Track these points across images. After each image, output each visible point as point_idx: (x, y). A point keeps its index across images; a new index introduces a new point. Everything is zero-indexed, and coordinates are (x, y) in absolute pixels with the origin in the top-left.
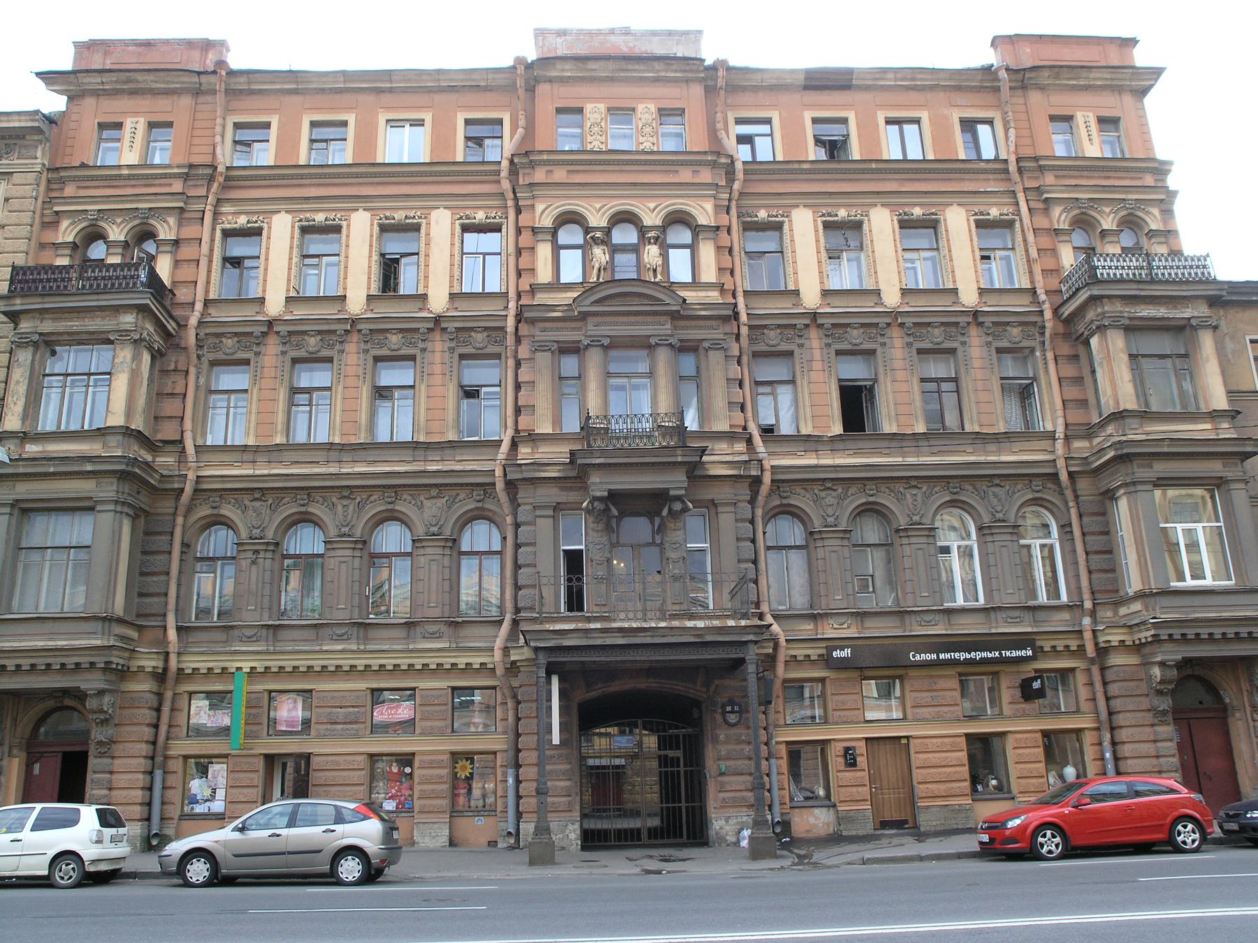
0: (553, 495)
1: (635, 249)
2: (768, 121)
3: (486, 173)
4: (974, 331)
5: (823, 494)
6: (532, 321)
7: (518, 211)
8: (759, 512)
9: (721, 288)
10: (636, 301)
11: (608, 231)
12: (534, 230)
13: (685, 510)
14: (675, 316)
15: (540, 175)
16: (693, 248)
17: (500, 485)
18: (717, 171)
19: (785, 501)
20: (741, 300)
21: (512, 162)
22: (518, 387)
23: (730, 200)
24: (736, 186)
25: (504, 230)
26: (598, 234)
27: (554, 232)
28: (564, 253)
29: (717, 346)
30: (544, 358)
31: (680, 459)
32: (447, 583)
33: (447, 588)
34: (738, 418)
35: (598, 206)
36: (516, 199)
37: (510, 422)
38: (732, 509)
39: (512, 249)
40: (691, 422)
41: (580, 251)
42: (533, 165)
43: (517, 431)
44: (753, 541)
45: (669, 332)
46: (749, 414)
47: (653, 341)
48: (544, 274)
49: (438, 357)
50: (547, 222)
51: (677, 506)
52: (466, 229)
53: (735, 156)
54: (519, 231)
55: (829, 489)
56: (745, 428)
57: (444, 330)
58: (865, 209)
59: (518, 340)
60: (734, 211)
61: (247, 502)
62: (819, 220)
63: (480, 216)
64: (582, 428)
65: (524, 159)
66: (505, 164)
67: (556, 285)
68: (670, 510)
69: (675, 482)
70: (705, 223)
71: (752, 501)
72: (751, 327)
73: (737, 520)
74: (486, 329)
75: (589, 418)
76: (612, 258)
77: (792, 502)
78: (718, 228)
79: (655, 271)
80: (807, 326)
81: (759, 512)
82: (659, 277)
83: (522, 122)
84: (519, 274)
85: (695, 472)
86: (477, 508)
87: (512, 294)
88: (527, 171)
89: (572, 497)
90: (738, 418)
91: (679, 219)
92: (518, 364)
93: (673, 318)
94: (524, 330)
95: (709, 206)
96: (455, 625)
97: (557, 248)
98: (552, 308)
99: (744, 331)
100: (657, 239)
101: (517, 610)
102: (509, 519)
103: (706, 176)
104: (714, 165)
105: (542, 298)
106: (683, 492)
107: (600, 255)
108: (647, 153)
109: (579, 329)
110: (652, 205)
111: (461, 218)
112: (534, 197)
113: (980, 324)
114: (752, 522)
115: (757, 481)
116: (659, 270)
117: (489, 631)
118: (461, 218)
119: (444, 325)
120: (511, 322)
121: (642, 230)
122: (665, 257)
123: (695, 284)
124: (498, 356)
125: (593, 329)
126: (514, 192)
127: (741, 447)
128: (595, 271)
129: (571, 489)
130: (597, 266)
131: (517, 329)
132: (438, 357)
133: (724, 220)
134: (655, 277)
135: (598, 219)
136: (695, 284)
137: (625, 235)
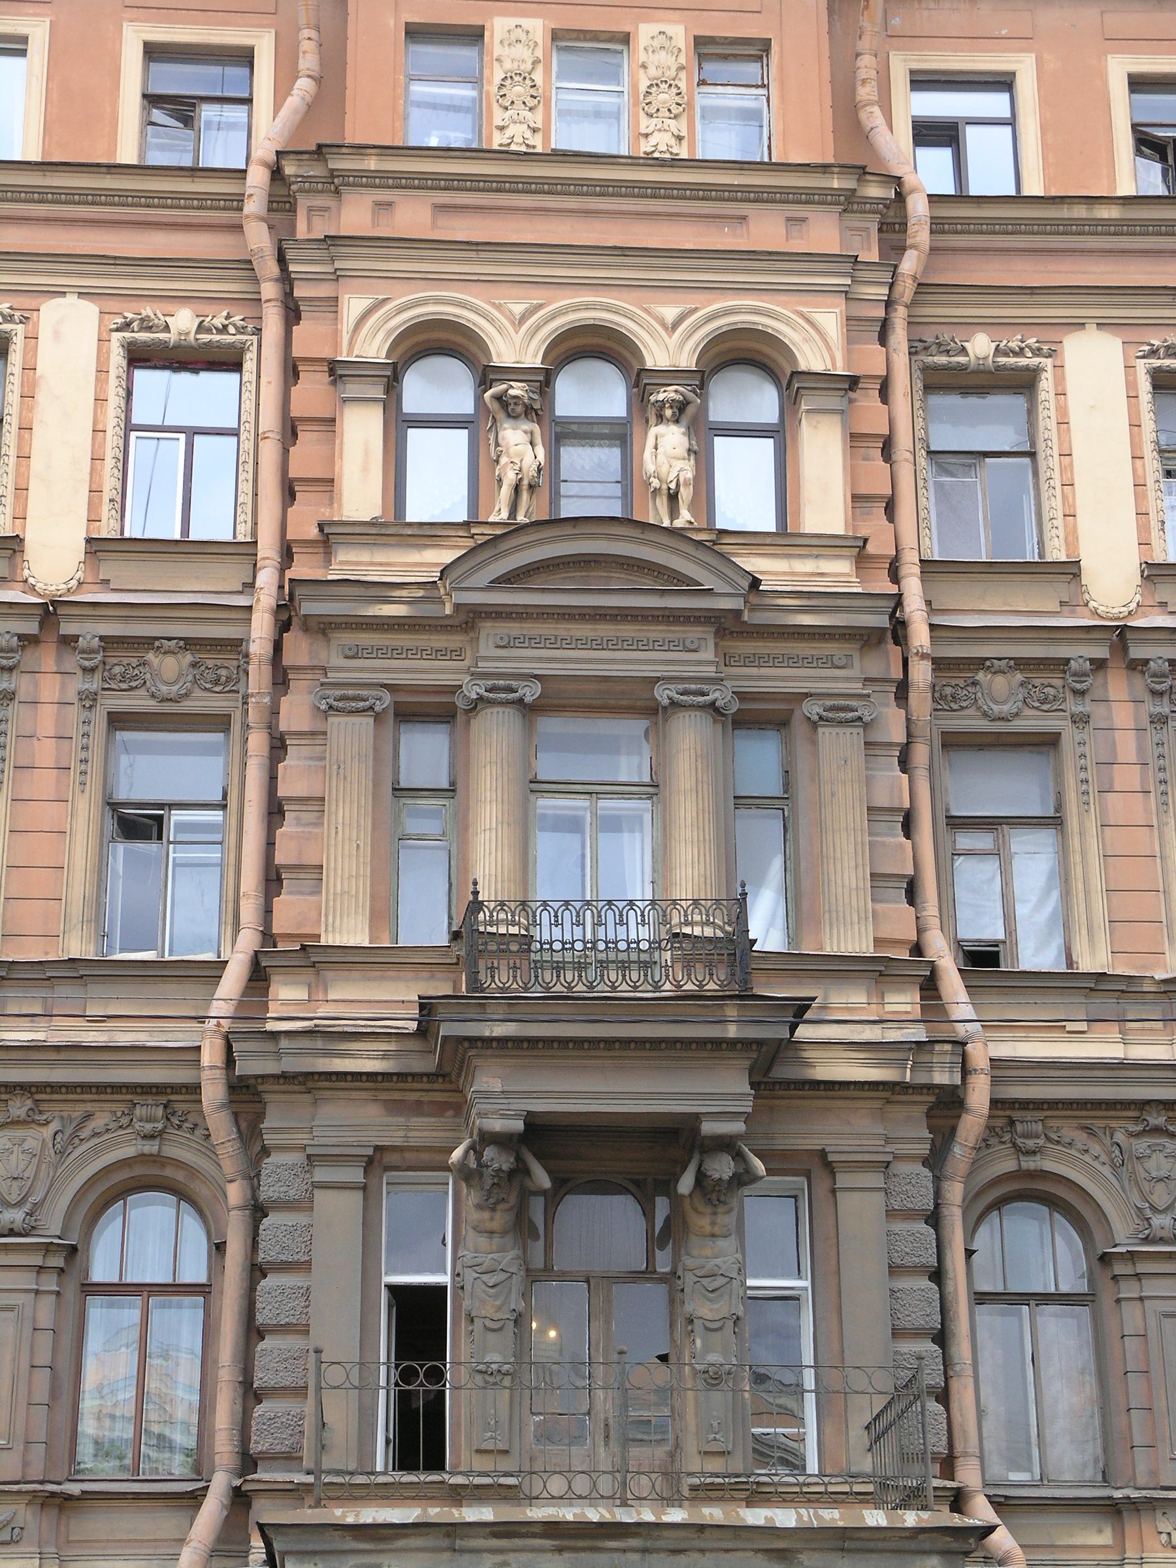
0: (365, 1122)
1: (618, 434)
2: (1003, 83)
3: (203, 201)
5: (1141, 1146)
6: (323, 628)
7: (292, 313)
8: (955, 1192)
9: (858, 550)
11: (544, 380)
12: (336, 371)
13: (743, 1178)
14: (726, 627)
15: (355, 215)
16: (781, 435)
17: (213, 1092)
18: (854, 221)
19: (1029, 1164)
20: (913, 588)
21: (276, 174)
22: (275, 811)
23: (889, 304)
24: (910, 264)
25: (249, 365)
26: (517, 389)
27: (392, 378)
28: (416, 437)
29: (842, 714)
30: (352, 734)
31: (732, 1031)
32: (42, 1378)
33: (41, 1393)
34: (899, 921)
35: (518, 309)
36: (286, 279)
37: (249, 911)
38: (876, 1180)
39: (270, 420)
40: (766, 928)
41: (464, 433)
42: (336, 185)
43: (268, 936)
44: (937, 1275)
45: (710, 671)
46: (931, 909)
47: (662, 694)
48: (360, 499)
49: (46, 720)
50: (373, 347)
51: (722, 1167)
52: (140, 357)
53: (909, 180)
54: (291, 370)
55: (1157, 1131)
56: (917, 949)
57: (69, 641)
59: (281, 678)
60: (899, 336)
62: (1142, 366)
63: (182, 323)
64: (456, 936)
65: (312, 167)
66: (258, 178)
67: (393, 529)
68: (701, 1177)
69: (717, 1096)
70: (818, 367)
71: (936, 1160)
72: (939, 664)
73: (891, 1214)
74: (189, 643)
75: (476, 906)
76: (554, 458)
77: (1049, 1165)
78: (853, 382)
79: (673, 497)
80: (1099, 665)
81: (955, 1192)
82: (685, 517)
83: (308, 61)
84: (289, 491)
85: (774, 1071)
86: (142, 1158)
87: (268, 549)
88: (319, 201)
89: (421, 1131)
90: (899, 921)
91: (743, 352)
92: (278, 747)
93: (722, 633)
94: (298, 650)
95: (830, 319)
96: (60, 1504)
97: (399, 425)
98: (382, 590)
99: (921, 673)
100: (681, 407)
101: (248, 1462)
102: (235, 1193)
103: (824, 233)
104: (849, 203)
105: (352, 562)
106: (738, 1127)
107: (520, 446)
108: (661, 163)
109: (457, 654)
110: (670, 313)
111: (126, 326)
112: (336, 277)
114: (934, 1219)
115: (947, 1104)
116: (685, 494)
117: (164, 1523)
118: (126, 326)
119: (68, 628)
120: (261, 629)
121: (641, 381)
122: (702, 458)
124: (221, 722)
125: (493, 652)
126: (282, 260)
127: (904, 1001)
128: (506, 492)
129: (418, 1108)
130: (510, 477)
131: (278, 647)
132: (46, 720)
133: (872, 360)
134: (674, 513)
135: (515, 347)
136: (785, 537)
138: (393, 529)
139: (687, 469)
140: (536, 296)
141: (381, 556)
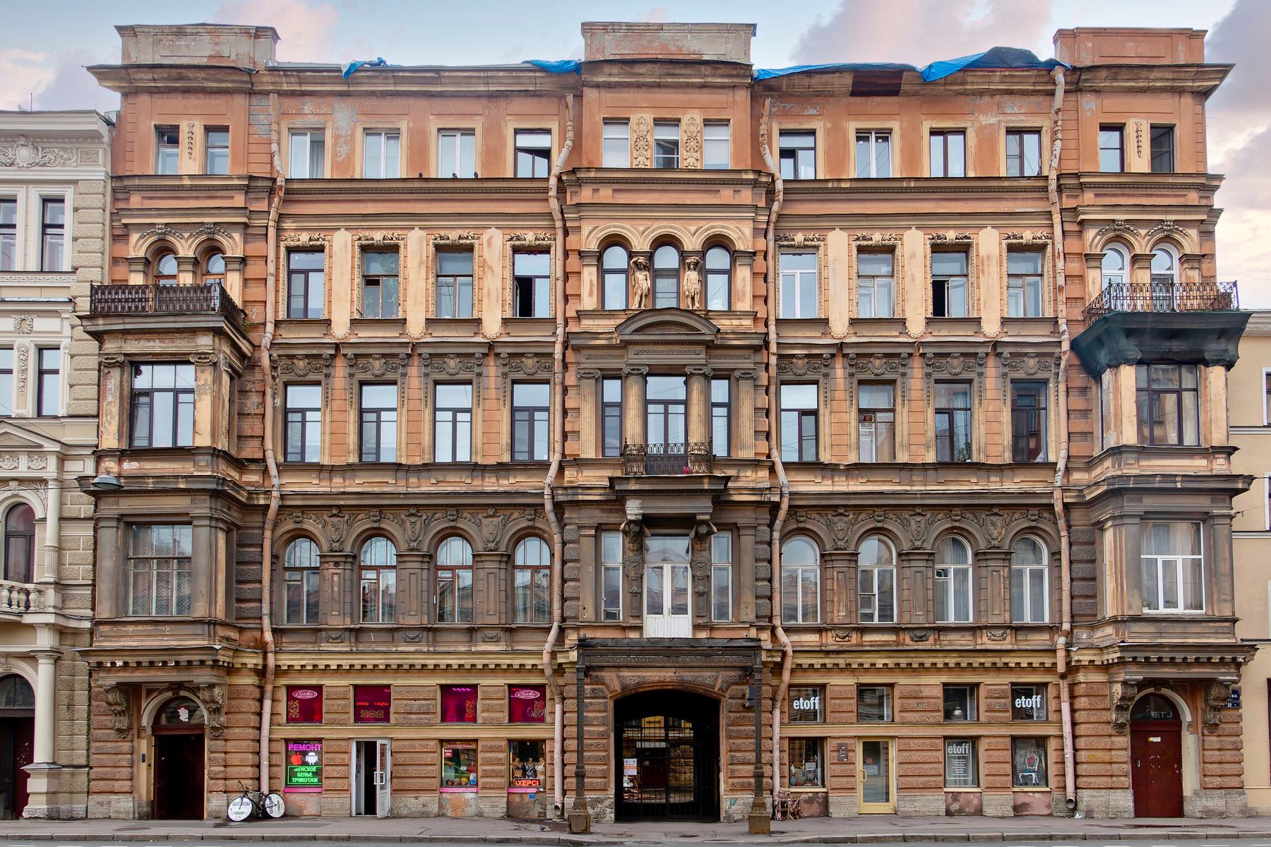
0: (598, 516)
1: (675, 274)
2: (812, 133)
3: (535, 191)
4: (991, 362)
5: (836, 519)
6: (577, 349)
7: (566, 233)
8: (776, 535)
9: (754, 316)
10: (674, 330)
11: (650, 256)
12: (581, 254)
13: (710, 533)
14: (710, 346)
15: (586, 195)
17: (549, 506)
18: (757, 191)
19: (801, 525)
20: (772, 328)
21: (559, 179)
22: (565, 412)
23: (768, 223)
24: (776, 207)
25: (552, 252)
26: (641, 260)
27: (600, 257)
29: (748, 376)
30: (589, 385)
31: (706, 487)
32: (503, 594)
33: (503, 599)
34: (763, 447)
35: (642, 229)
36: (564, 220)
37: (558, 447)
38: (752, 532)
39: (560, 274)
40: (720, 450)
42: (580, 183)
43: (564, 455)
44: (770, 562)
45: (703, 362)
46: (774, 442)
47: (688, 370)
48: (589, 303)
49: (492, 380)
50: (593, 246)
51: (703, 530)
52: (516, 250)
53: (777, 175)
54: (566, 254)
55: (841, 514)
56: (769, 456)
57: (497, 355)
58: (900, 232)
59: (565, 366)
60: (771, 235)
61: (325, 517)
62: (855, 244)
63: (529, 237)
64: (621, 455)
65: (572, 178)
66: (553, 182)
67: (601, 312)
68: (697, 533)
69: (702, 508)
71: (771, 525)
72: (780, 357)
73: (757, 543)
74: (536, 355)
75: (626, 446)
76: (654, 284)
77: (807, 526)
78: (754, 254)
79: (693, 298)
80: (833, 356)
81: (776, 535)
82: (697, 305)
83: (570, 134)
84: (566, 298)
85: (720, 500)
86: (528, 527)
87: (560, 320)
88: (574, 189)
89: (612, 518)
90: (763, 447)
91: (718, 242)
92: (565, 390)
93: (708, 348)
94: (571, 356)
95: (747, 229)
96: (510, 631)
97: (602, 272)
98: (596, 335)
99: (773, 360)
100: (696, 264)
101: (563, 619)
102: (557, 538)
103: (746, 196)
104: (755, 184)
105: (587, 324)
106: (707, 517)
107: (642, 278)
108: (690, 171)
109: (622, 357)
110: (693, 229)
111: (511, 239)
112: (580, 219)
113: (999, 355)
114: (770, 544)
115: (775, 507)
116: (697, 298)
117: (540, 636)
118: (511, 239)
119: (498, 350)
120: (558, 349)
121: (683, 255)
122: (704, 283)
123: (730, 313)
124: (547, 382)
125: (634, 357)
126: (562, 213)
127: (764, 474)
128: (637, 298)
129: (611, 511)
131: (564, 355)
132: (492, 380)
133: (761, 244)
134: (693, 304)
136: (730, 313)
137: (667, 258)
138: (601, 312)
139: (698, 286)
140: (649, 223)
141: (597, 322)
